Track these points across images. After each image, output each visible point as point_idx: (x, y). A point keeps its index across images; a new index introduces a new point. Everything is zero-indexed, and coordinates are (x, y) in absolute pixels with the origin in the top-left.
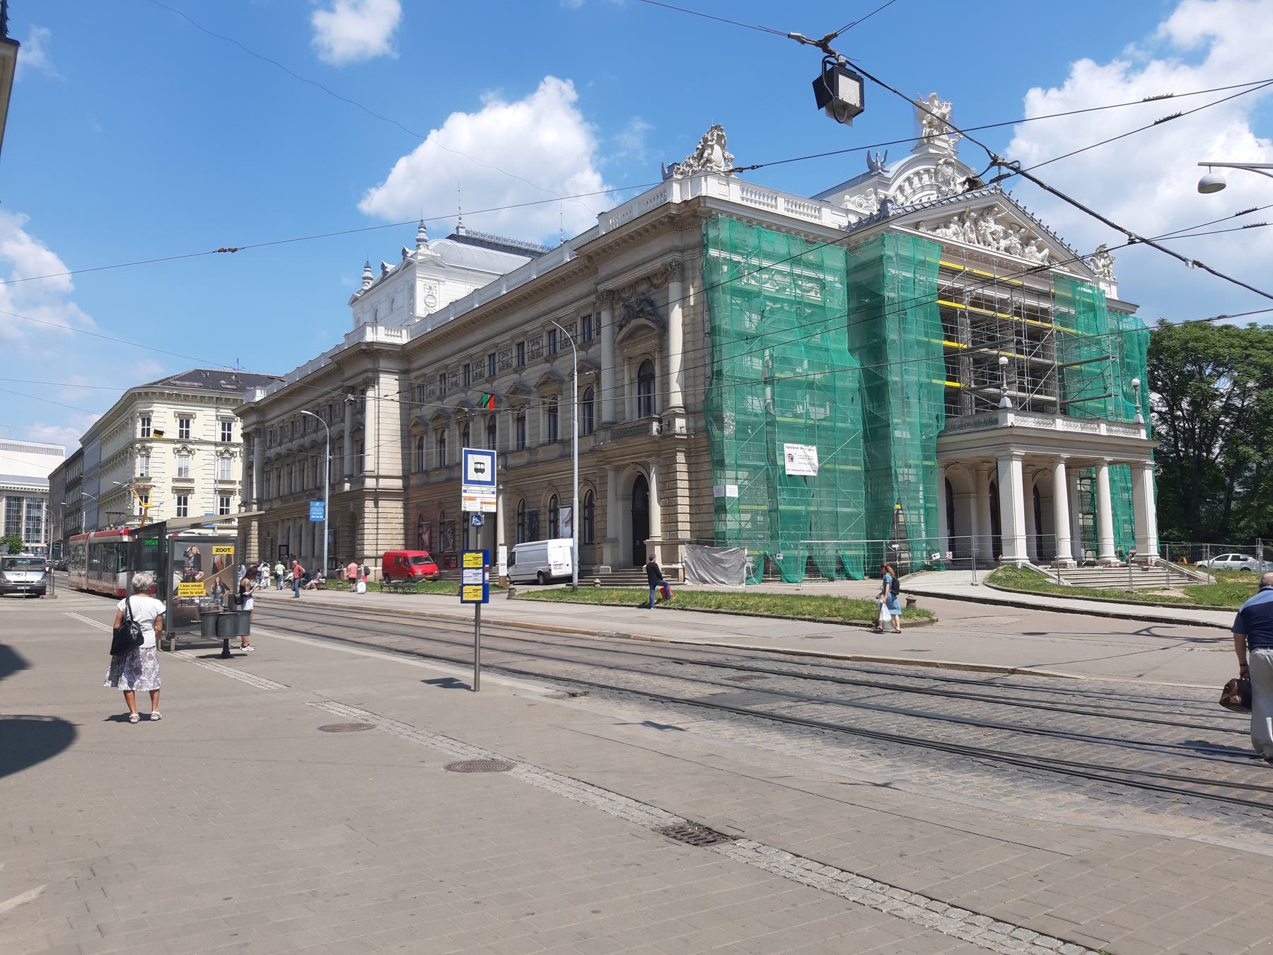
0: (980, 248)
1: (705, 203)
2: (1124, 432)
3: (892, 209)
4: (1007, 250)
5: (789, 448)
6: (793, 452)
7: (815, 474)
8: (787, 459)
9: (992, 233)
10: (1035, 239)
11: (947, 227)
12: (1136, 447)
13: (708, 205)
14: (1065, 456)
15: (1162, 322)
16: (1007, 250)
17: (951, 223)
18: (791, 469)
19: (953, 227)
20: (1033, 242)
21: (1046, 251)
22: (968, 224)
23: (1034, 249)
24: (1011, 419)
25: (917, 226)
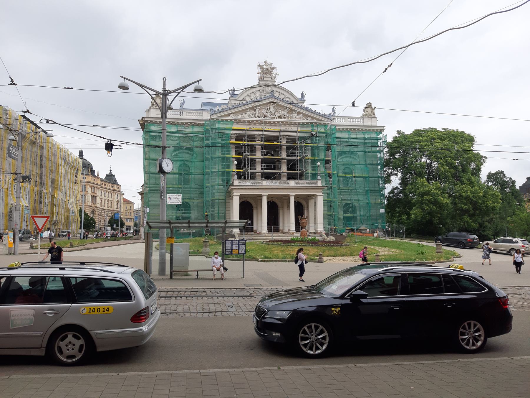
0: (262, 119)
1: (145, 119)
2: (307, 183)
3: (213, 112)
4: (280, 117)
5: (169, 196)
6: (171, 197)
7: (181, 204)
8: (168, 199)
9: (270, 112)
10: (295, 111)
11: (246, 114)
12: (317, 188)
13: (145, 120)
14: (267, 193)
15: (399, 132)
16: (280, 117)
17: (247, 112)
18: (169, 202)
19: (248, 113)
20: (295, 112)
21: (302, 114)
22: (257, 110)
23: (296, 114)
24: (236, 183)
25: (229, 115)
